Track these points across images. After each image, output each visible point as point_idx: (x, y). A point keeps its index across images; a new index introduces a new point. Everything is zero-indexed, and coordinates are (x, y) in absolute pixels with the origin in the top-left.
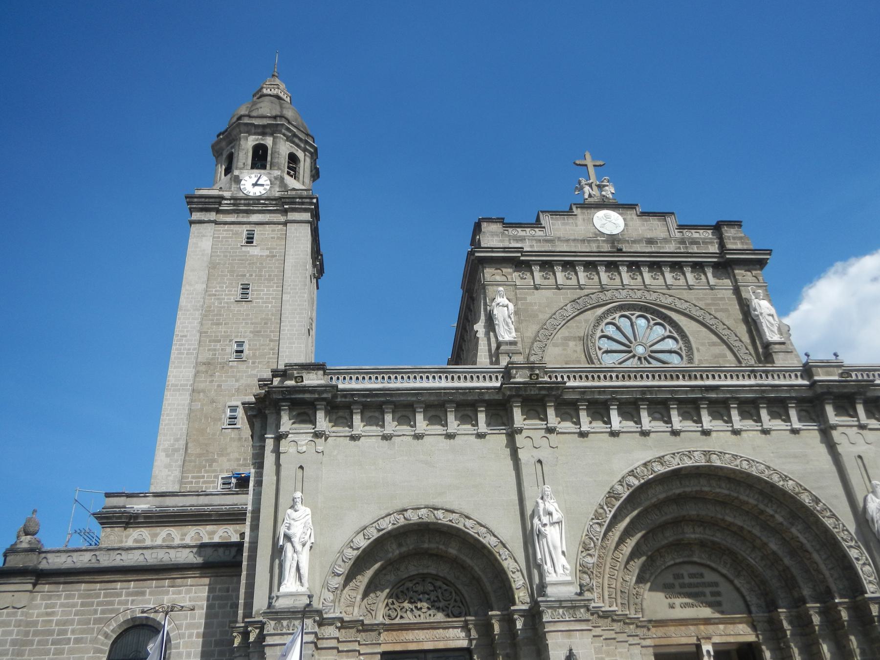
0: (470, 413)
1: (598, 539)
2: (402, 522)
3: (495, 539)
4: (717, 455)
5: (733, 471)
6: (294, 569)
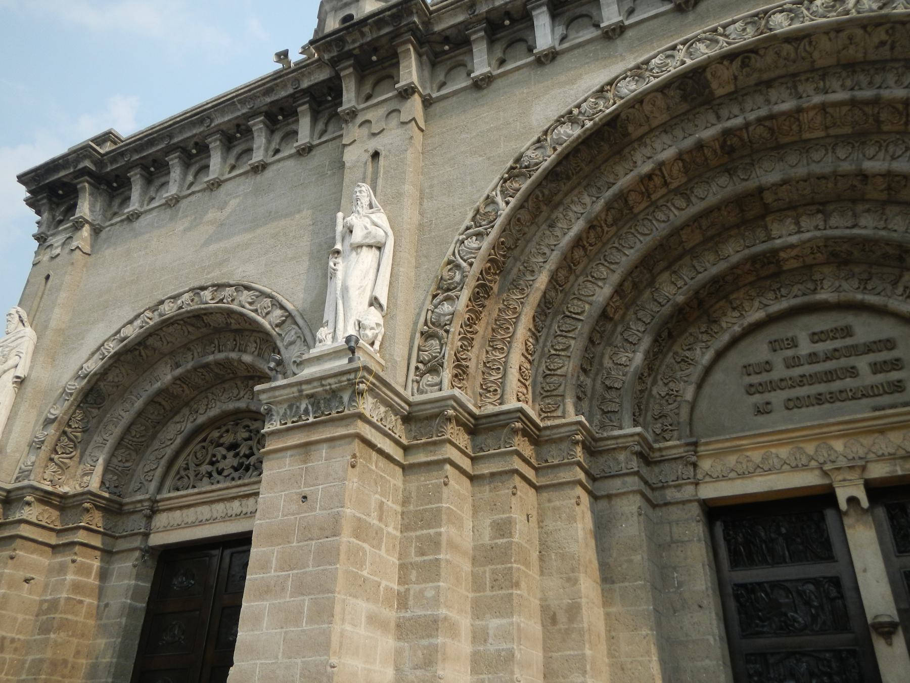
1: (471, 265)
2: (157, 319)
3: (278, 312)
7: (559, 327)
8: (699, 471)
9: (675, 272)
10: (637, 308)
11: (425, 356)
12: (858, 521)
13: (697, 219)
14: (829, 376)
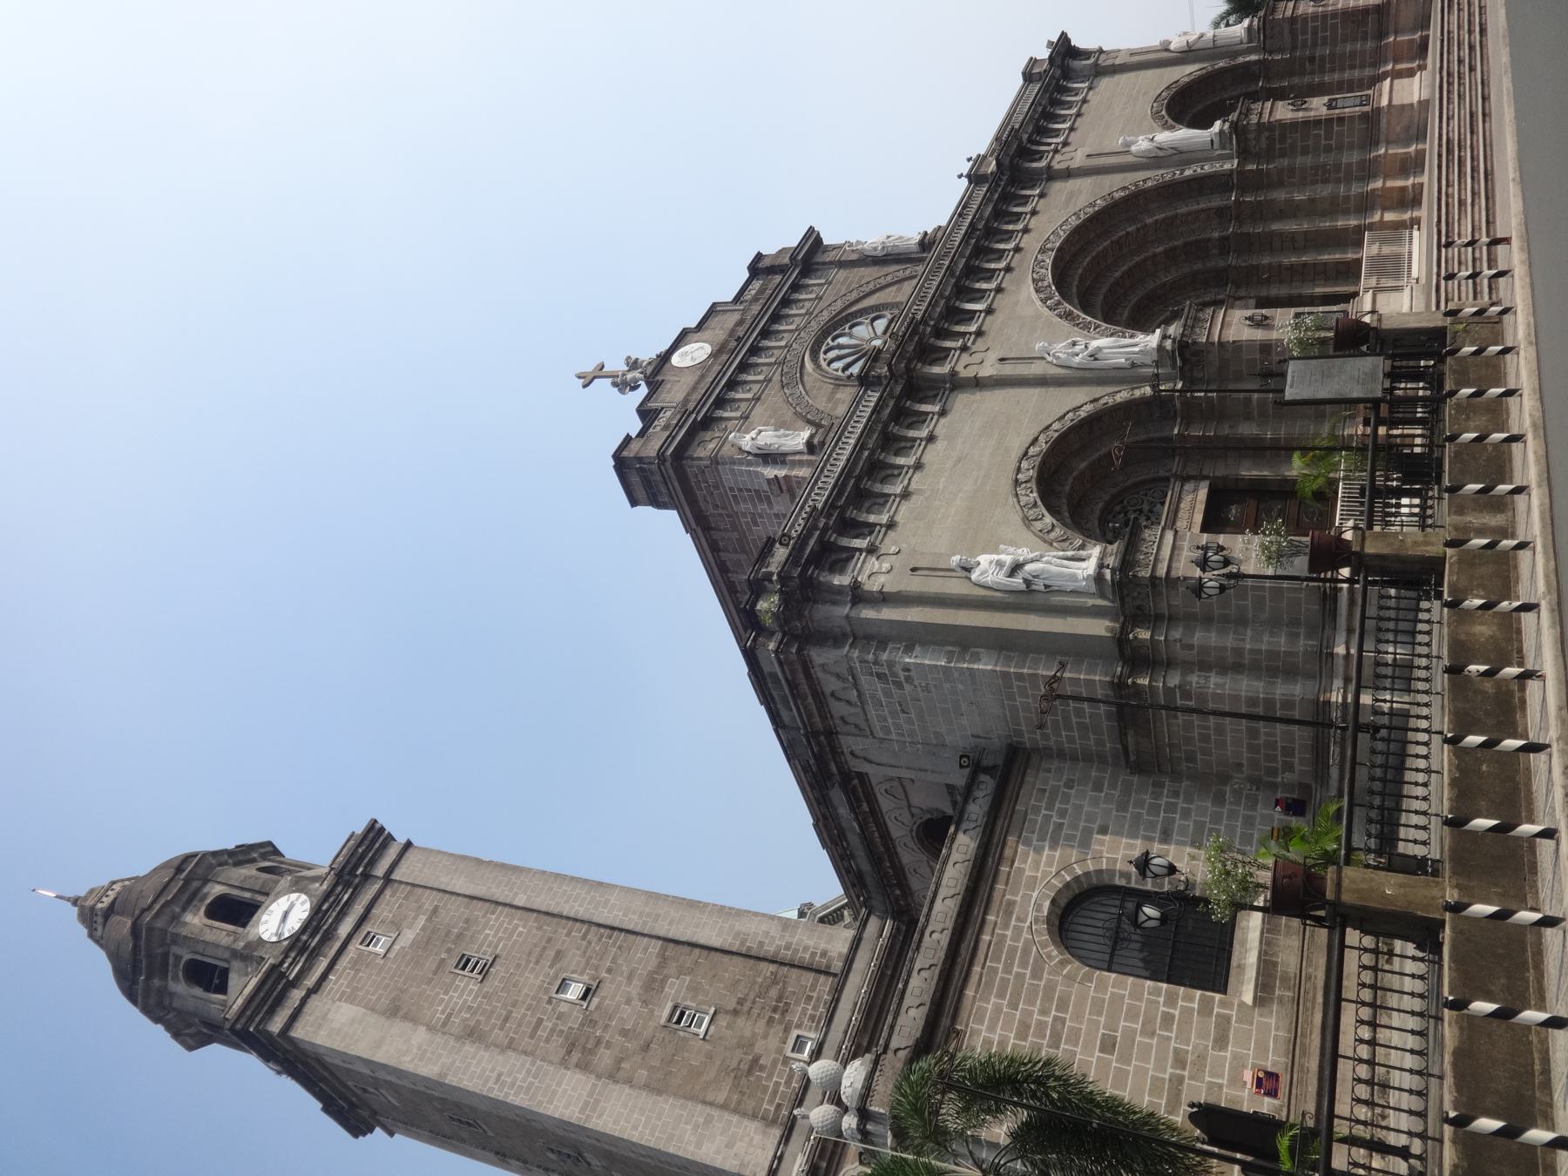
0: (910, 421)
5: (1067, 241)
6: (1065, 562)
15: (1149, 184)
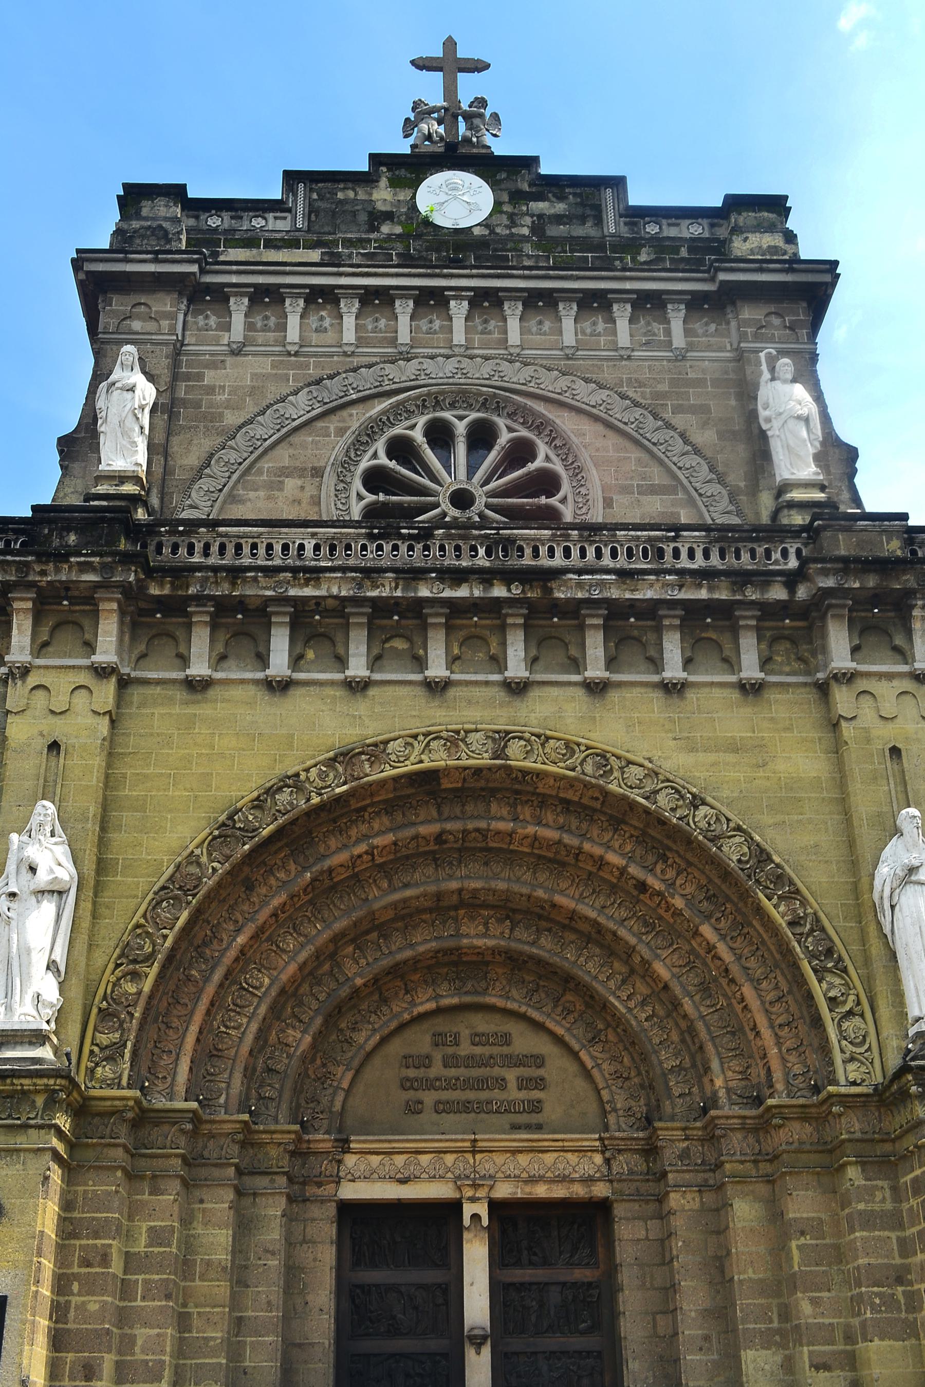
4: (528, 741)
7: (232, 999)
8: (342, 1168)
9: (359, 948)
10: (314, 981)
11: (104, 1039)
12: (476, 1236)
13: (394, 905)
14: (481, 1084)
15: (779, 914)
